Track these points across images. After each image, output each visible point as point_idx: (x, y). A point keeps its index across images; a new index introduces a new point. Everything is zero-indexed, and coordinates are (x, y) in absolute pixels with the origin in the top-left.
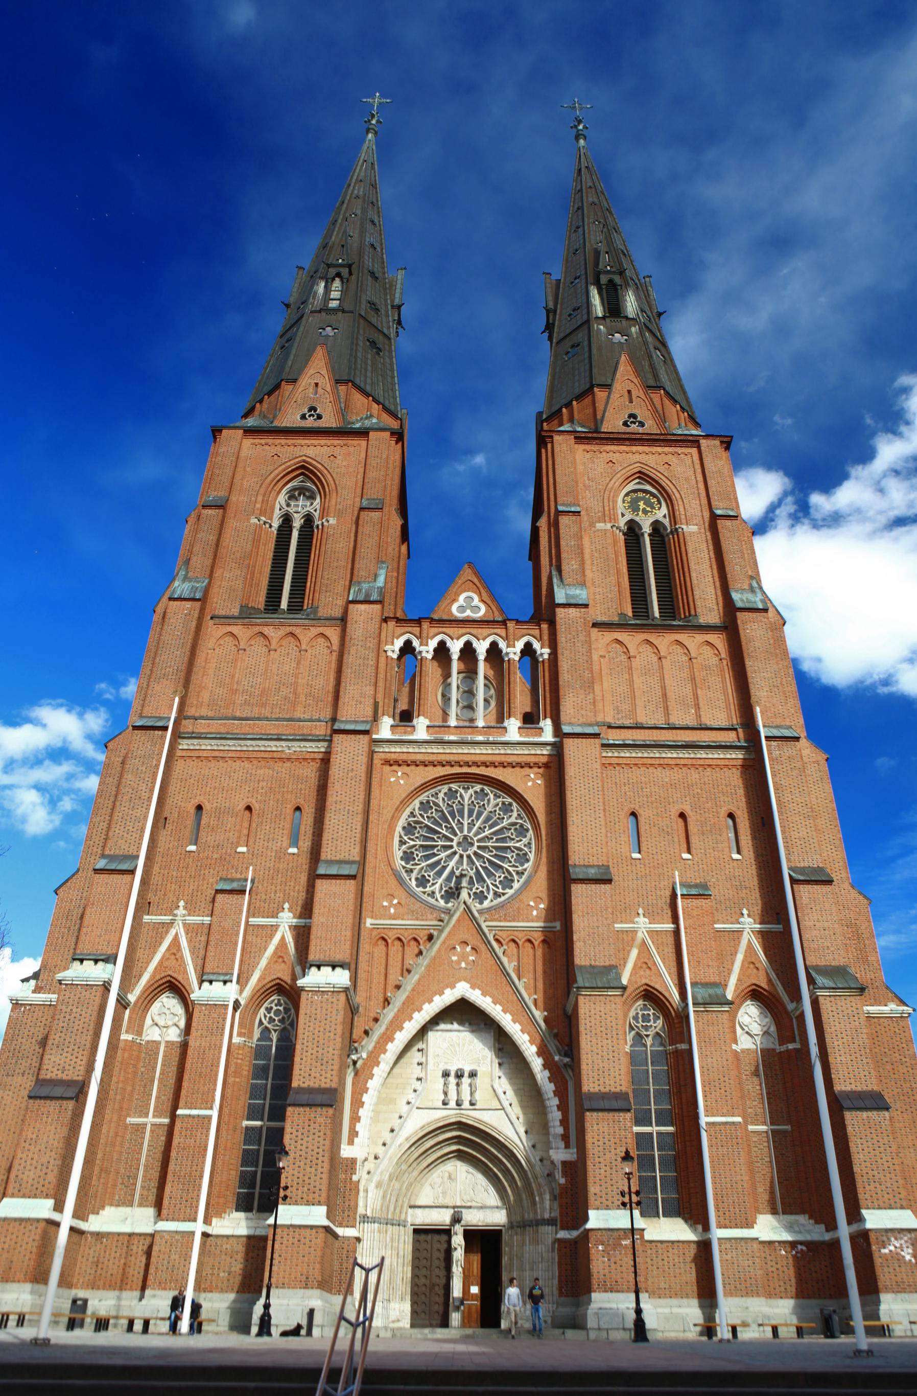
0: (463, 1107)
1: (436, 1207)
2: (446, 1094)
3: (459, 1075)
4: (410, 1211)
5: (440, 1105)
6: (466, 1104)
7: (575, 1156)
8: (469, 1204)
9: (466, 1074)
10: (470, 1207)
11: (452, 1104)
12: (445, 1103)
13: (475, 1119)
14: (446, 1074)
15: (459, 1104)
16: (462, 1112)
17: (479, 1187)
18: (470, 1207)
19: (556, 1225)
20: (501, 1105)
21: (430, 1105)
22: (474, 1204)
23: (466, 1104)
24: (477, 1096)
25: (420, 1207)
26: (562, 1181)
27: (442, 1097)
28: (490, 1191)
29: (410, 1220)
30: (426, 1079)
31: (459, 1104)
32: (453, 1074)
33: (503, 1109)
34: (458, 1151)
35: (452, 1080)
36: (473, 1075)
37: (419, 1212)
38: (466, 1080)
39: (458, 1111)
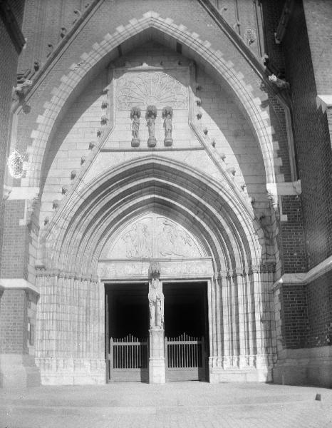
0: (156, 148)
1: (129, 261)
2: (135, 133)
3: (151, 114)
4: (101, 265)
5: (130, 147)
6: (160, 145)
7: (299, 190)
8: (167, 257)
9: (159, 114)
10: (170, 260)
11: (144, 145)
12: (135, 145)
13: (171, 161)
14: (135, 114)
15: (152, 146)
16: (155, 153)
17: (180, 239)
18: (170, 260)
19: (274, 272)
20: (203, 144)
21: (116, 146)
22: (173, 256)
23: (160, 145)
24: (174, 135)
25: (111, 261)
26: (284, 218)
27: (131, 137)
28: (192, 243)
29: (100, 274)
30: (112, 120)
31: (152, 146)
32: (143, 114)
33: (204, 148)
34: (154, 200)
35: (143, 120)
36: (167, 114)
37: (111, 267)
38: (159, 120)
39: (151, 153)
